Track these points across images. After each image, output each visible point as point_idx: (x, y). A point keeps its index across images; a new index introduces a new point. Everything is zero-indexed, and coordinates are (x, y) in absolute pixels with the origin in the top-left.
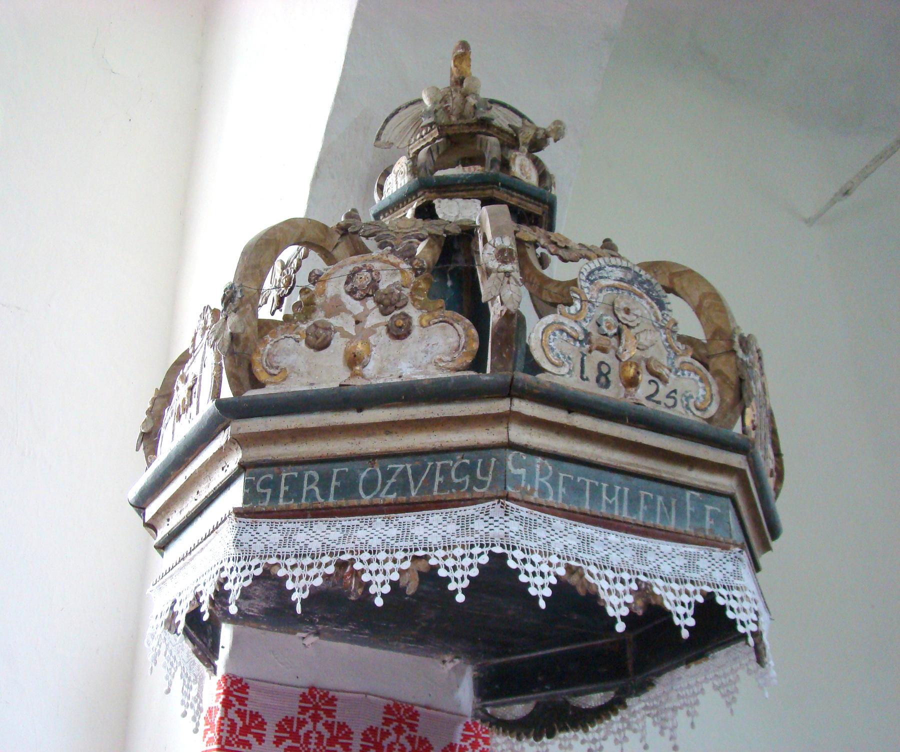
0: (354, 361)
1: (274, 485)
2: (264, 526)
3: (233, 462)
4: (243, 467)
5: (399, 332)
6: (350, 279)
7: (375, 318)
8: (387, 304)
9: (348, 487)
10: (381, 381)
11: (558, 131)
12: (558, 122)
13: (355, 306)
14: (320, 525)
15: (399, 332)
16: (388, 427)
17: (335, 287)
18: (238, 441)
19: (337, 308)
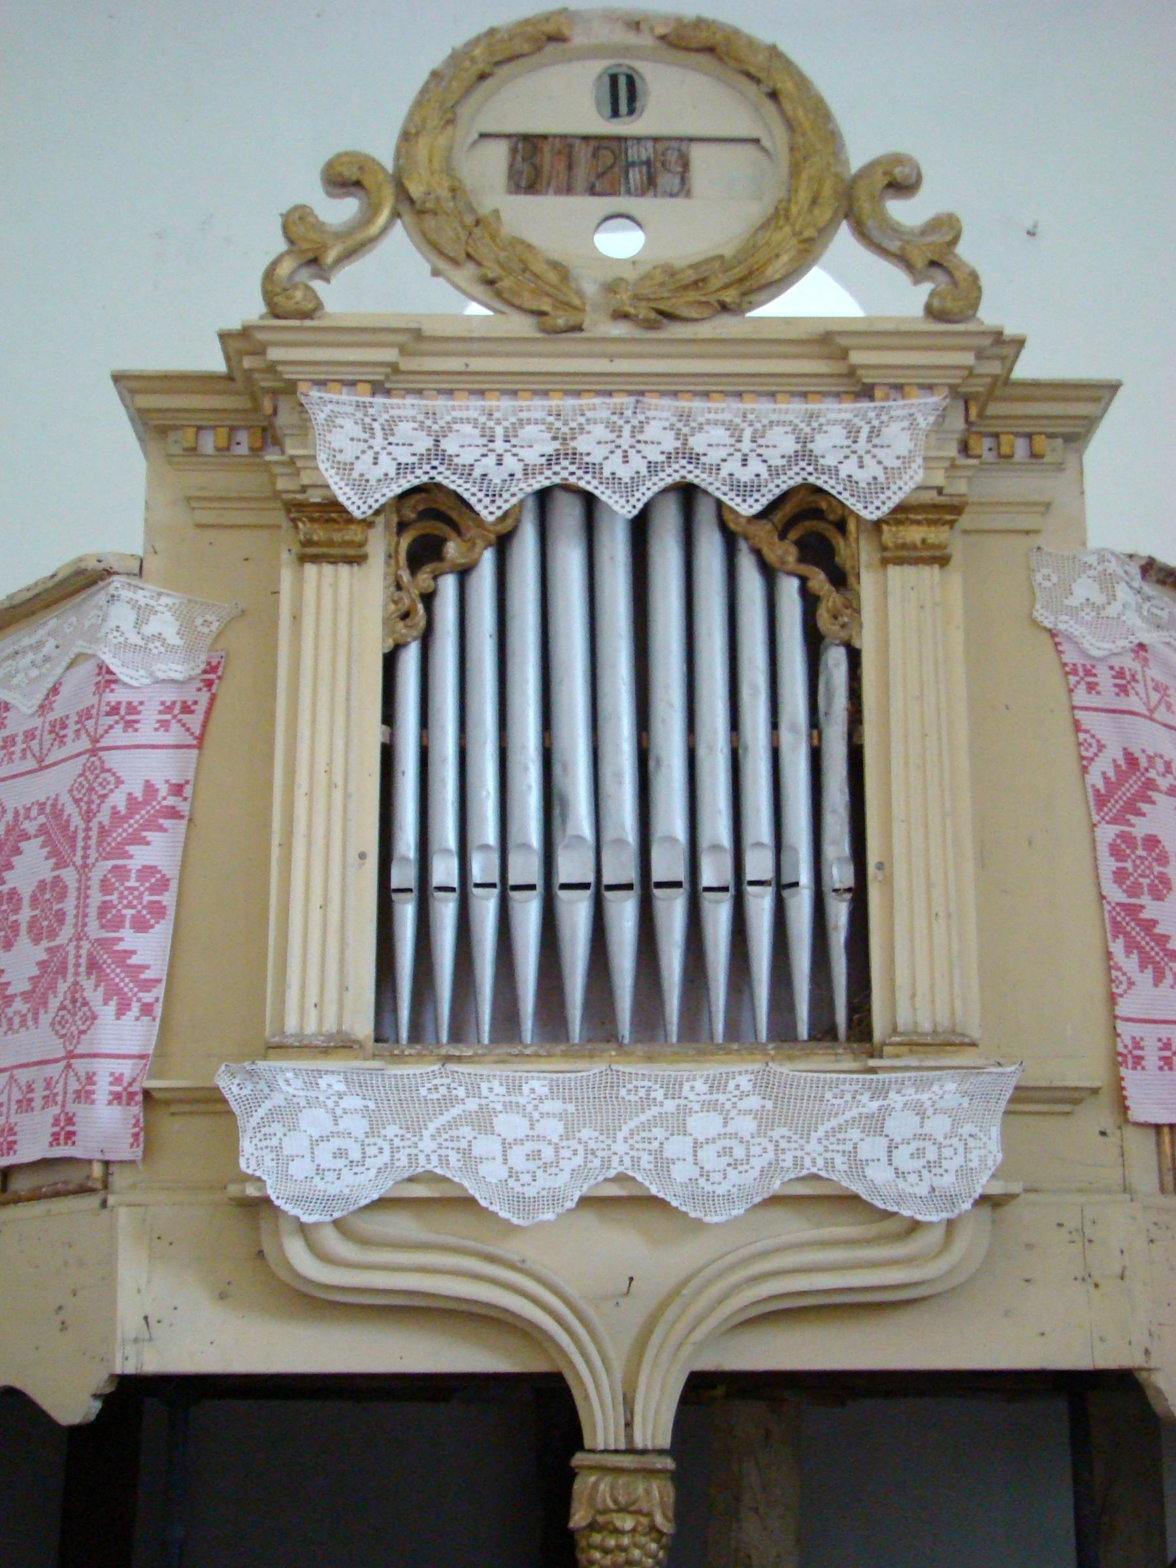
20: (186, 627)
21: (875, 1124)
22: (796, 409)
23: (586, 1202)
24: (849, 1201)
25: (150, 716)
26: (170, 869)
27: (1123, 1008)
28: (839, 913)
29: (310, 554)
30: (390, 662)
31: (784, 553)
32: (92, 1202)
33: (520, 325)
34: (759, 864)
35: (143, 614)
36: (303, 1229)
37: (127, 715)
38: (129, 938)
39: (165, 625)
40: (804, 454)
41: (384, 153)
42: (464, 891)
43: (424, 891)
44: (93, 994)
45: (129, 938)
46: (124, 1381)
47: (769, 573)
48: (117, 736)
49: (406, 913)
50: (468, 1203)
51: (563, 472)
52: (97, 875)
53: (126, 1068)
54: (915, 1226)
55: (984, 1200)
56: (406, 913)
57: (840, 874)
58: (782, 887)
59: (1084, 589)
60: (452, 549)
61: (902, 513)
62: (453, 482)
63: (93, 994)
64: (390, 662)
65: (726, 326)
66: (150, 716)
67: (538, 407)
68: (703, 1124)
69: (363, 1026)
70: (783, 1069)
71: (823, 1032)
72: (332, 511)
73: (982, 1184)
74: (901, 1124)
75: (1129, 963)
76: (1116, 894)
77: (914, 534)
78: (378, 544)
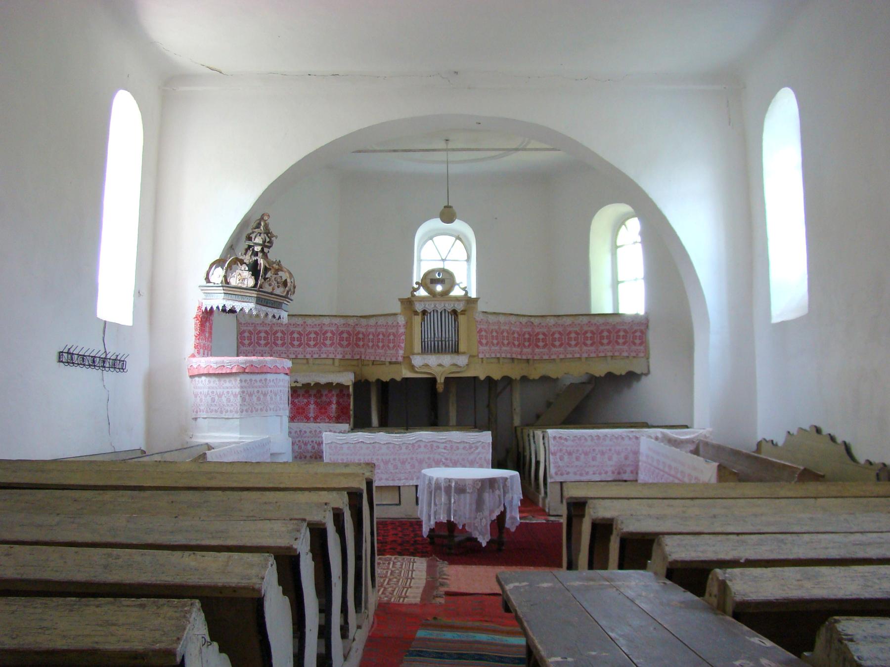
0: (273, 289)
1: (259, 300)
2: (258, 306)
3: (256, 296)
4: (256, 297)
5: (278, 287)
6: (275, 278)
7: (276, 284)
8: (278, 283)
9: (267, 303)
10: (275, 293)
11: (276, 237)
12: (277, 236)
13: (274, 282)
14: (264, 307)
15: (278, 287)
16: (273, 298)
17: (273, 279)
18: (257, 294)
19: (273, 282)
20: (404, 318)
21: (458, 360)
22: (453, 302)
23: (438, 365)
24: (457, 365)
25: (402, 326)
26: (404, 338)
27: (480, 349)
28: (457, 343)
29: (415, 315)
30: (422, 323)
31: (453, 313)
32: (399, 365)
33: (431, 296)
34: (450, 339)
35: (401, 318)
36: (417, 368)
37: (400, 326)
38: (401, 344)
39: (403, 319)
40: (454, 306)
41: (420, 282)
42: (428, 341)
43: (425, 341)
44: (399, 349)
45: (401, 344)
46: (403, 378)
47: (452, 315)
48: (399, 328)
49: (423, 343)
50: (428, 365)
51: (435, 308)
52: (398, 339)
53: (402, 354)
54: (460, 367)
55: (467, 365)
56: (423, 343)
57: (457, 340)
58: (452, 340)
59: (477, 314)
60: (426, 314)
61: (462, 311)
62: (426, 309)
63: (399, 349)
64: (422, 323)
65: (447, 296)
66: (402, 326)
67: (433, 303)
68: (446, 360)
69: (420, 352)
70: (452, 355)
71: (455, 352)
72: (417, 311)
73: (466, 363)
74: (460, 359)
75: (479, 345)
76: (479, 340)
77: (462, 312)
78: (420, 314)
